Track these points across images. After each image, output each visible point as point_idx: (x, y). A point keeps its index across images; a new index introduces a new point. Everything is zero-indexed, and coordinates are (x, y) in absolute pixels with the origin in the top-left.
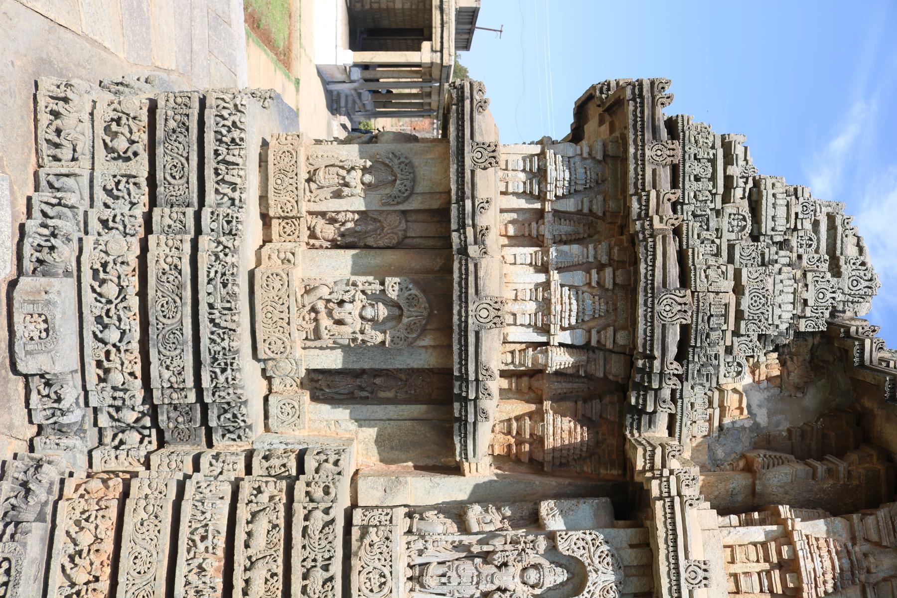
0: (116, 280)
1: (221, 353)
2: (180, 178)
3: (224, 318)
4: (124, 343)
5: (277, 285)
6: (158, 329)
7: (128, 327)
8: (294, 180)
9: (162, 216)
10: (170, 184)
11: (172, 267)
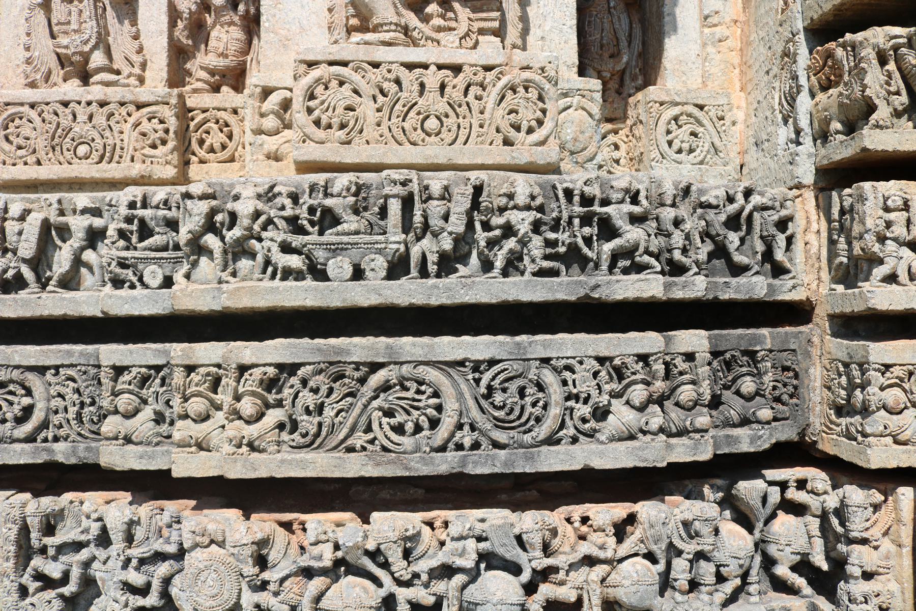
0: (318, 583)
1: (552, 236)
2: (29, 393)
3: (436, 222)
4: (521, 557)
5: (341, 96)
6: (476, 446)
7: (471, 544)
8: (79, 110)
9: (128, 440)
10: (45, 425)
11: (271, 398)
